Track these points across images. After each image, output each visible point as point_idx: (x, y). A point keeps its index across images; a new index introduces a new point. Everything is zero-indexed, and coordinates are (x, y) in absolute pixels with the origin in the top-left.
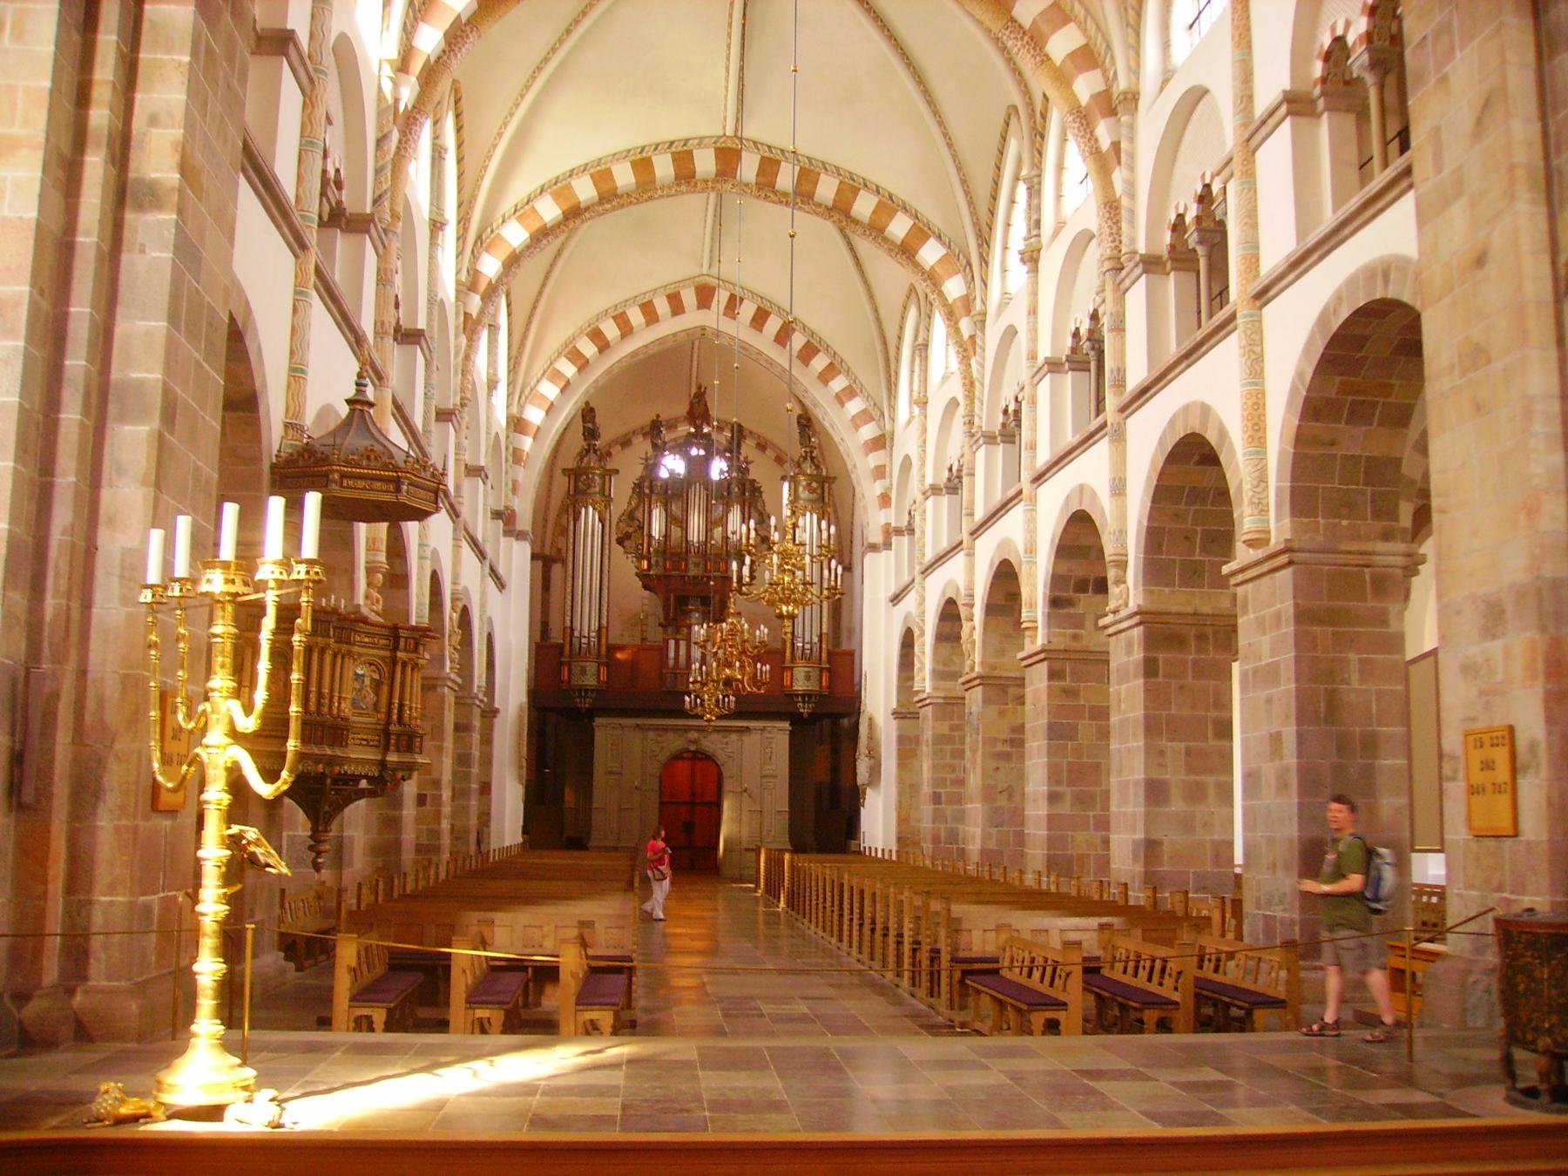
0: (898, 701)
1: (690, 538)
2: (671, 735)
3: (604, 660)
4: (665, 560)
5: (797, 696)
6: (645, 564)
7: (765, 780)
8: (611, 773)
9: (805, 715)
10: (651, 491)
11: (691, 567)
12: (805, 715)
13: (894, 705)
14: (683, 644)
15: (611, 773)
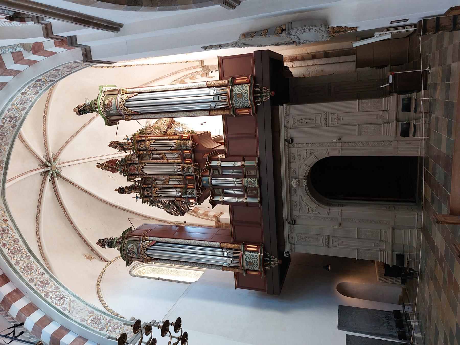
0: (216, 4)
1: (173, 173)
2: (295, 199)
3: (241, 246)
4: (188, 189)
5: (256, 103)
6: (192, 200)
7: (330, 123)
8: (328, 243)
9: (273, 94)
10: (151, 197)
11: (189, 173)
12: (273, 94)
13: (218, 8)
14: (227, 191)
15: (328, 243)
